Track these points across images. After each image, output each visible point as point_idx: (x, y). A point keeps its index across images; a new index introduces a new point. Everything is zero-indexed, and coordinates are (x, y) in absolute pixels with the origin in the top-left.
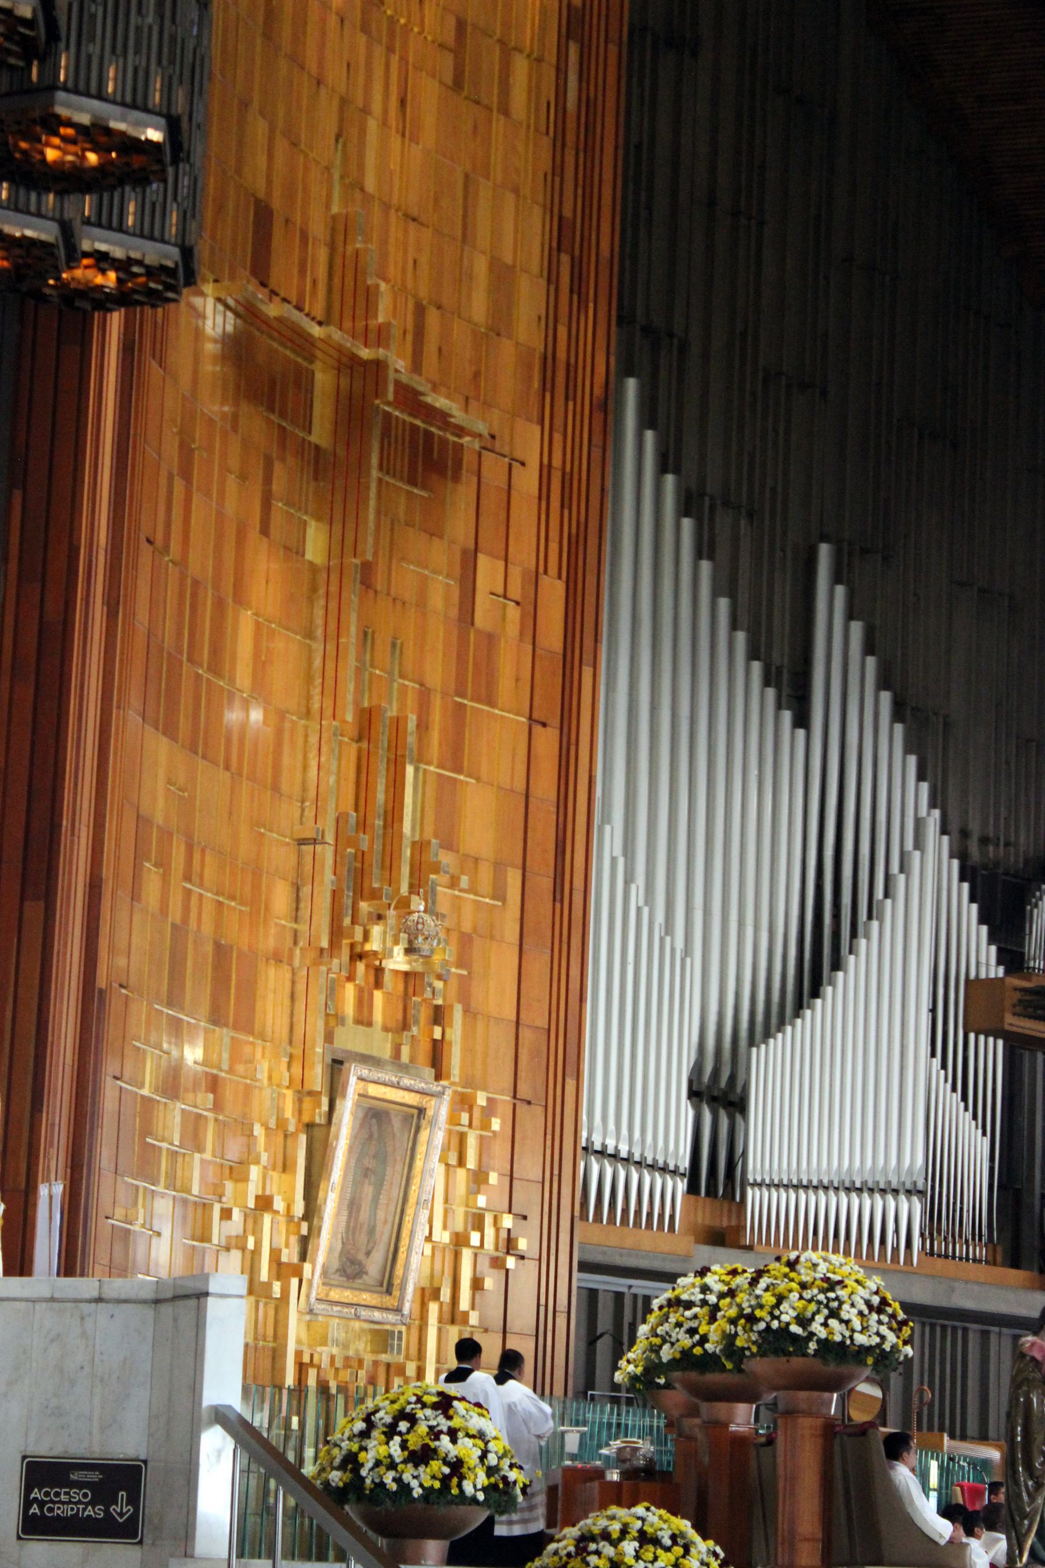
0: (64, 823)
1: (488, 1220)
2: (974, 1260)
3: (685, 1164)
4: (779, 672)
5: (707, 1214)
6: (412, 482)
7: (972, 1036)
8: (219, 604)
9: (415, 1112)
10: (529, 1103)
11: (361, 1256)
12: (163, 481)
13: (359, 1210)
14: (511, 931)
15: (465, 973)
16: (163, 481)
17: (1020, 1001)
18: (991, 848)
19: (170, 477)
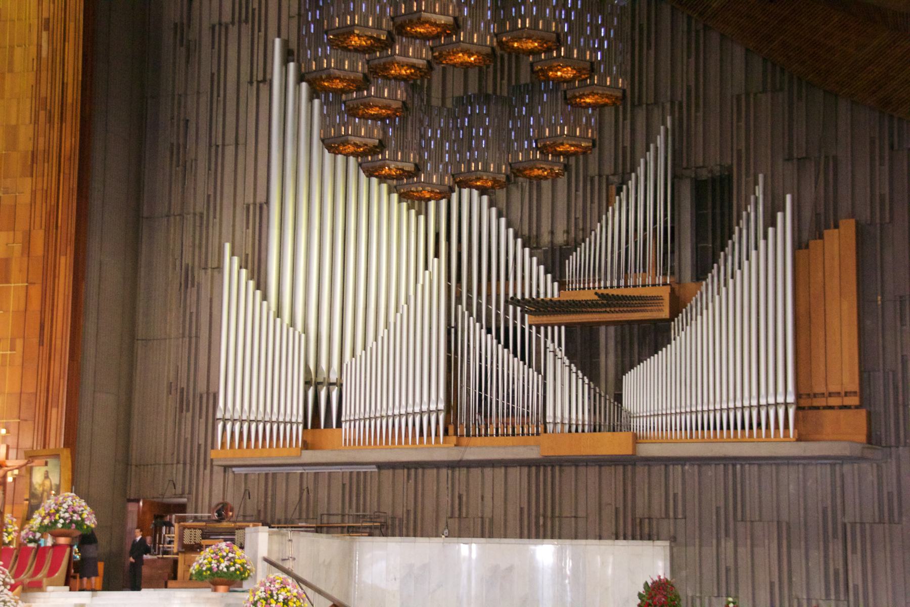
2: (528, 435)
10: (26, 420)
14: (18, 361)
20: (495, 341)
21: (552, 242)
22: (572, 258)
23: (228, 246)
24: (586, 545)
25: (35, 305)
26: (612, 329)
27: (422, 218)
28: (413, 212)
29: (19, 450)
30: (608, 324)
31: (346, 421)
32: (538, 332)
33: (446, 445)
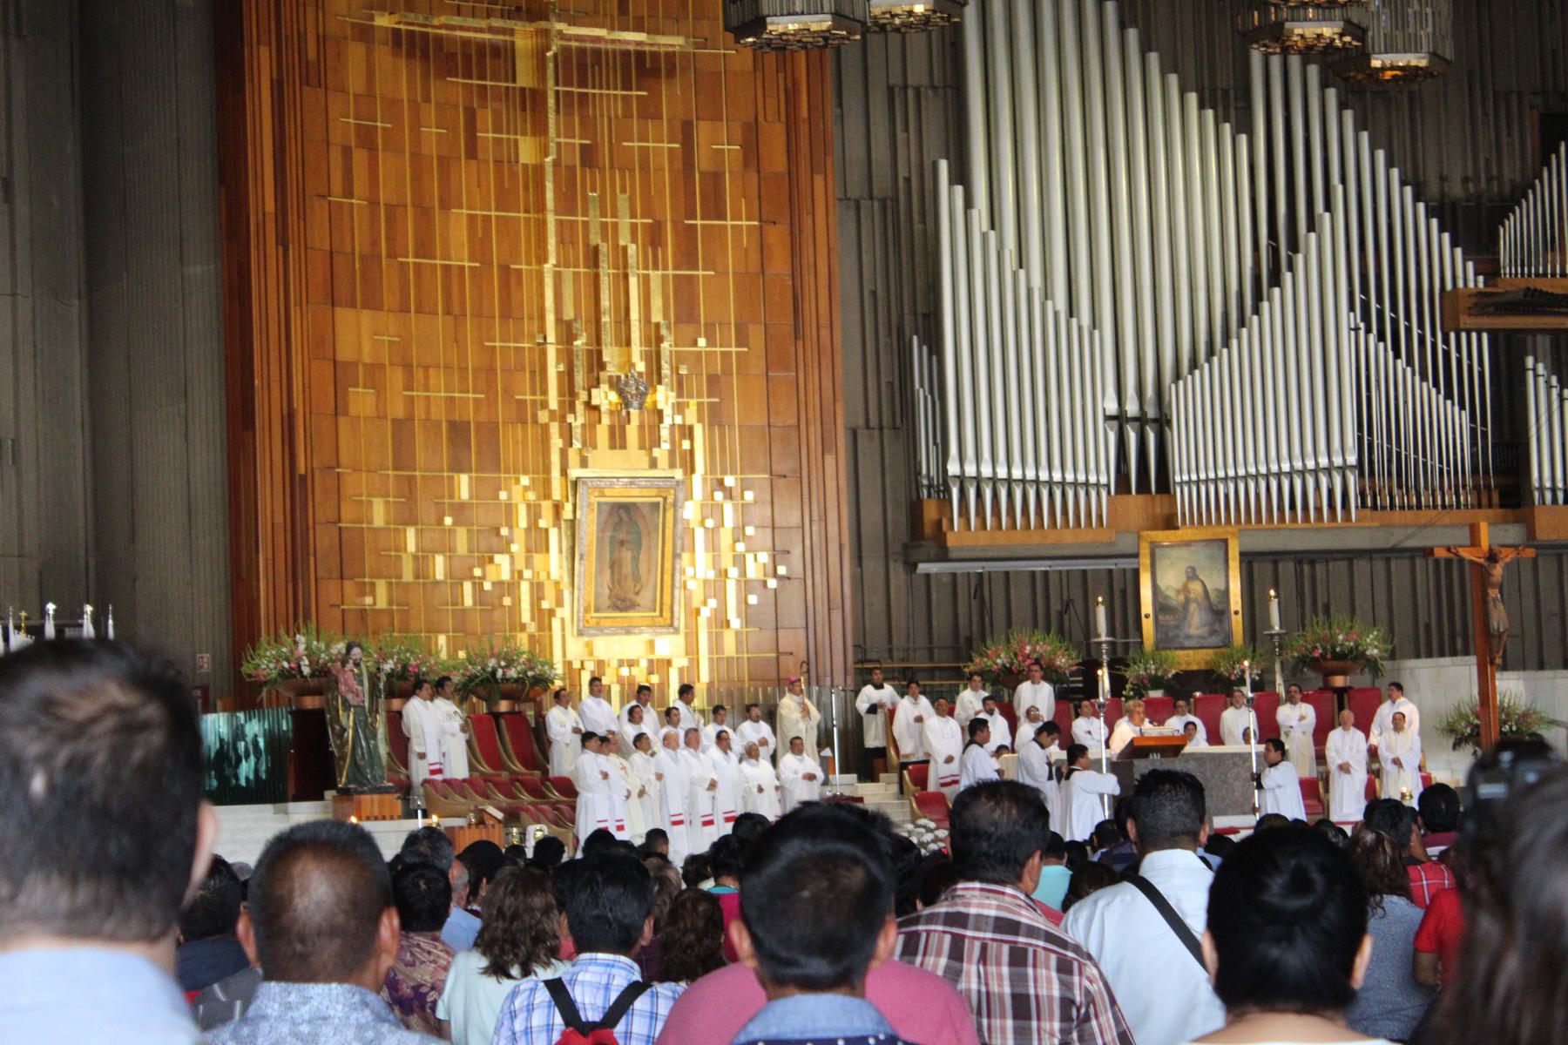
0: (256, 382)
1: (750, 557)
3: (1108, 476)
4: (1225, 92)
5: (1159, 505)
6: (627, 87)
7: (1452, 336)
8: (424, 213)
9: (661, 500)
11: (631, 595)
12: (336, 155)
13: (620, 566)
14: (757, 367)
15: (717, 400)
16: (336, 155)
17: (1476, 305)
18: (1471, 185)
19: (347, 152)
20: (1391, 354)
21: (1443, 195)
22: (1510, 222)
23: (943, 165)
24: (1554, 678)
25: (780, 265)
26: (1547, 340)
27: (1243, 138)
28: (1227, 128)
29: (776, 532)
30: (1543, 331)
31: (1181, 484)
32: (1446, 341)
33: (1359, 524)
